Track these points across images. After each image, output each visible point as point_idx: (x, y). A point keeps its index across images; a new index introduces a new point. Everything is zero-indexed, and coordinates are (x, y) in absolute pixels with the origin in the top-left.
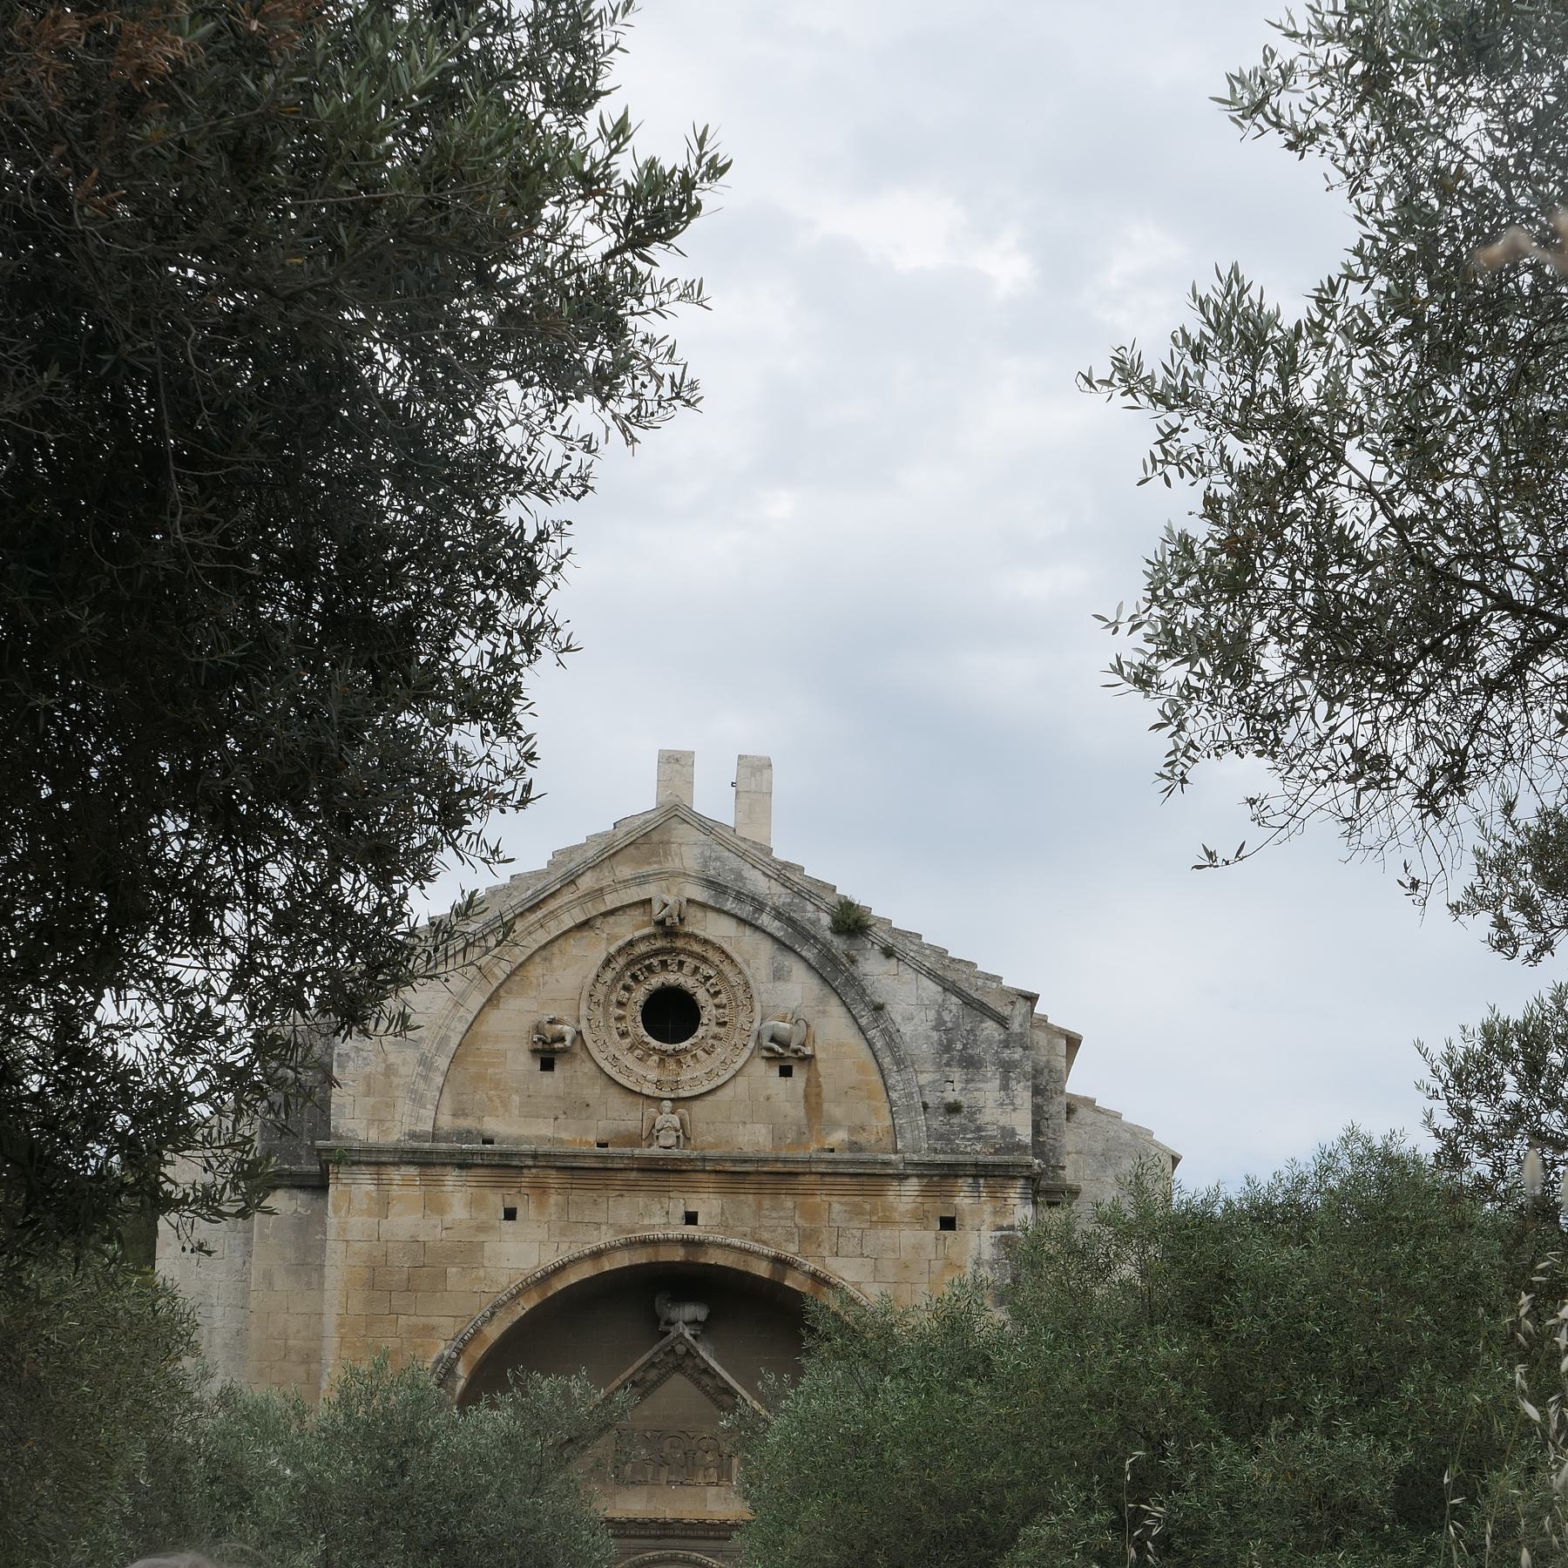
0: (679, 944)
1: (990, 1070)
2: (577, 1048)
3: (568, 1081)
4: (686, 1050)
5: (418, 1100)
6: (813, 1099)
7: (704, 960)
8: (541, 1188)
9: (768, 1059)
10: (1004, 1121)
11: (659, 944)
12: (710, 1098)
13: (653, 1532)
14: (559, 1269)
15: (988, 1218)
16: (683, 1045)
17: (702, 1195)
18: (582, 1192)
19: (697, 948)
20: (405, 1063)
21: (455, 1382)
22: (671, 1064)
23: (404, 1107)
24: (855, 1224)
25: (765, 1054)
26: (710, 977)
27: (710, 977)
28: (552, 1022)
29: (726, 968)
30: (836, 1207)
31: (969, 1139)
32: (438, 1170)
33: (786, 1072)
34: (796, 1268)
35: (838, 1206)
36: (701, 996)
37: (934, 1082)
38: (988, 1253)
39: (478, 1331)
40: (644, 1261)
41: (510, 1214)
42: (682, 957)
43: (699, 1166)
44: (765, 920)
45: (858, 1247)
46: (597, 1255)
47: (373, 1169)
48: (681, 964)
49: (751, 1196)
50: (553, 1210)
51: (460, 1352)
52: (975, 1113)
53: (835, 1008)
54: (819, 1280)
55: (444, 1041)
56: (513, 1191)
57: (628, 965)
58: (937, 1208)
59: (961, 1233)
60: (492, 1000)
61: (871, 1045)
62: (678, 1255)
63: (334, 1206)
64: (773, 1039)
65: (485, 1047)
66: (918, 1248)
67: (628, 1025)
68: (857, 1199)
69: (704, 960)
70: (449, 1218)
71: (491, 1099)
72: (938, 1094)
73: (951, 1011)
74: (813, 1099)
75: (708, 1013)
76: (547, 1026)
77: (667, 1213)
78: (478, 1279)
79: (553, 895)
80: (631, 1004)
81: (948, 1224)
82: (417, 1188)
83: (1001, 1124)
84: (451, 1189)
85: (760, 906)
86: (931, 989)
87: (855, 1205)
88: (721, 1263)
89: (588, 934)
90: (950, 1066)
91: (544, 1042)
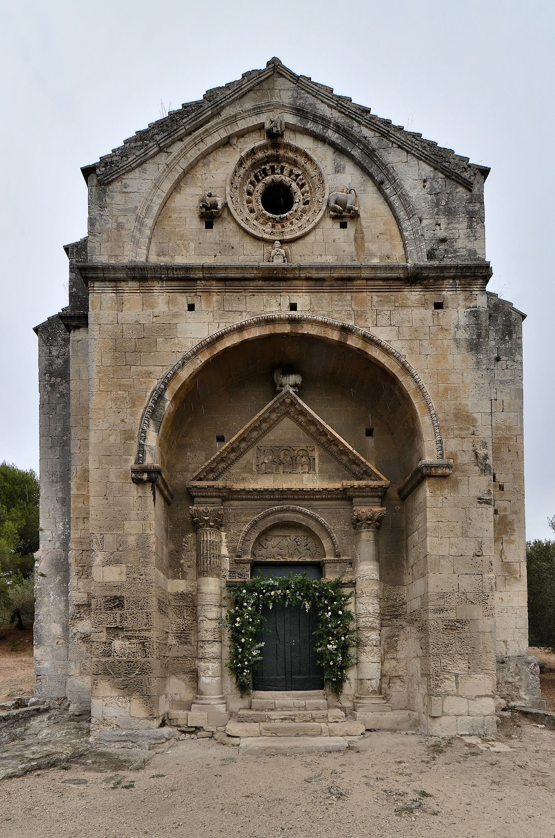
0: (281, 152)
2: (225, 215)
3: (221, 234)
4: (286, 219)
5: (136, 243)
7: (295, 163)
8: (209, 292)
10: (469, 246)
11: (270, 152)
12: (301, 242)
14: (220, 338)
15: (462, 303)
16: (285, 215)
17: (299, 294)
18: (231, 294)
19: (291, 155)
21: (164, 403)
22: (279, 226)
23: (128, 247)
24: (386, 308)
25: (332, 213)
26: (299, 175)
27: (299, 175)
28: (210, 195)
29: (308, 166)
30: (375, 299)
31: (449, 258)
32: (150, 283)
33: (343, 226)
34: (353, 333)
37: (429, 225)
38: (463, 321)
39: (175, 374)
40: (267, 333)
41: (191, 308)
42: (283, 164)
44: (331, 134)
45: (389, 321)
46: (241, 329)
47: (113, 284)
48: (282, 169)
49: (326, 294)
51: (166, 385)
52: (453, 242)
53: (371, 188)
54: (368, 339)
55: (149, 208)
57: (254, 166)
58: (432, 297)
59: (447, 310)
60: (176, 187)
61: (390, 205)
62: (286, 329)
64: (336, 203)
66: (422, 320)
67: (254, 205)
68: (387, 294)
69: (295, 163)
70: (156, 311)
72: (432, 232)
73: (438, 183)
75: (298, 197)
76: (207, 197)
77: (280, 305)
78: (174, 344)
79: (207, 121)
80: (255, 192)
81: (439, 306)
82: (138, 294)
83: (468, 248)
84: (158, 294)
86: (426, 170)
87: (386, 297)
88: (311, 332)
89: (229, 149)
90: (439, 215)
91: (207, 208)
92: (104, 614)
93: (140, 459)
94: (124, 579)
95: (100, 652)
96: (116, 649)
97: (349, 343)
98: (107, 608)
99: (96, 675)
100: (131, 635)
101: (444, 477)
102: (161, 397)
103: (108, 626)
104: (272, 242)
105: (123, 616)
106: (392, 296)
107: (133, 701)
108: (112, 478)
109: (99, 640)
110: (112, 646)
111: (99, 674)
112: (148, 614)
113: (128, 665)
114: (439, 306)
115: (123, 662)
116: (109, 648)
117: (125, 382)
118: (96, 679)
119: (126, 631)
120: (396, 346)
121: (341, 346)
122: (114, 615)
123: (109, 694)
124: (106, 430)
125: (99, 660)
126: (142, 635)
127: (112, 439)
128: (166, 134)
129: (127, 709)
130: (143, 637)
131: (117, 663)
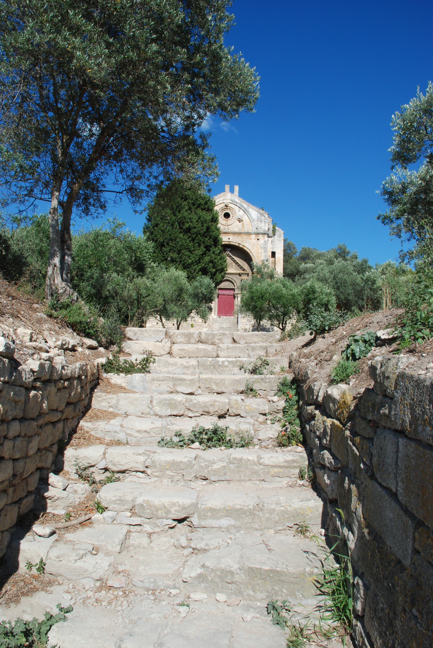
1: (263, 222)
6: (243, 225)
35: (245, 237)
36: (230, 213)
62: (227, 243)
74: (243, 225)
85: (237, 203)
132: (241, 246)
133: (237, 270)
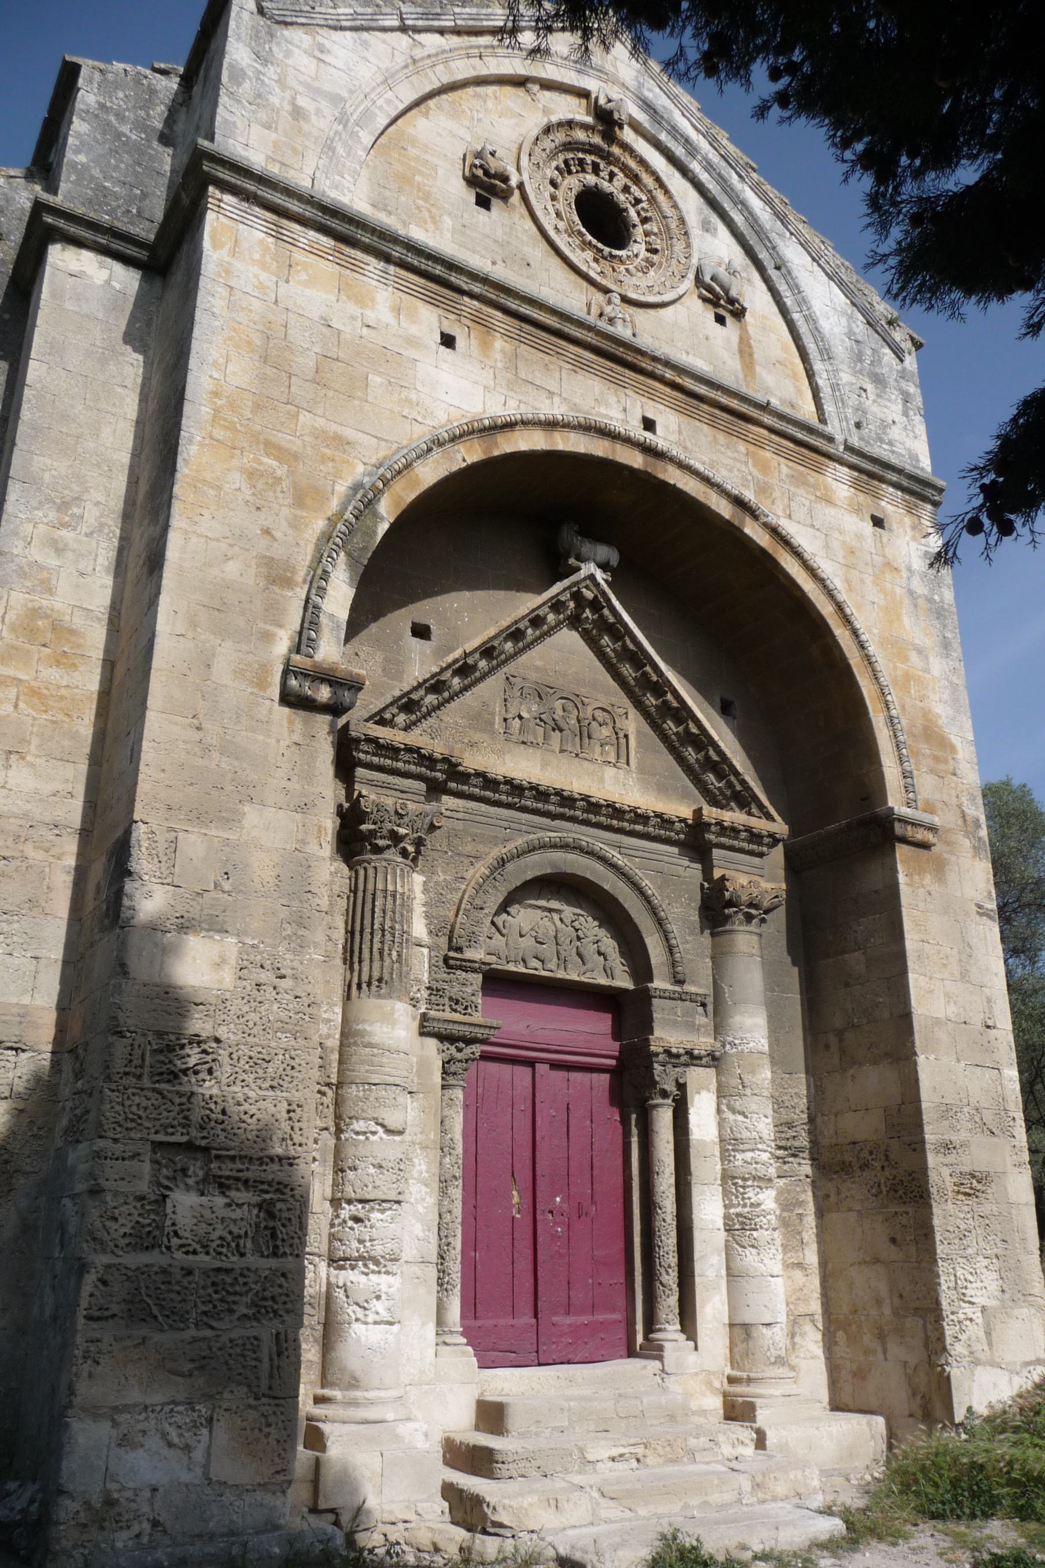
9: (705, 300)
11: (597, 140)
13: (552, 808)
14: (509, 426)
18: (533, 350)
19: (632, 164)
20: (318, 111)
33: (720, 320)
42: (616, 170)
43: (660, 369)
46: (551, 425)
48: (612, 175)
50: (498, 356)
56: (452, 317)
57: (569, 146)
63: (213, 237)
65: (413, 151)
67: (561, 206)
69: (636, 179)
70: (371, 316)
71: (418, 208)
78: (408, 401)
87: (801, 473)
88: (680, 485)
91: (486, 173)
92: (149, 1094)
93: (303, 642)
94: (228, 978)
95: (123, 1230)
96: (179, 1219)
97: (747, 530)
98: (162, 1074)
99: (99, 1319)
100: (234, 1174)
101: (925, 846)
102: (370, 504)
103: (161, 1137)
104: (606, 291)
105: (213, 1106)
106: (813, 477)
107: (222, 1423)
108: (222, 672)
109: (123, 1187)
110: (169, 1209)
111: (106, 1318)
112: (294, 1107)
113: (214, 1284)
114: (878, 522)
115: (197, 1272)
116: (152, 1216)
117: (283, 439)
118: (97, 1335)
119: (218, 1157)
120: (826, 568)
121: (732, 533)
122: (184, 1100)
123: (135, 1396)
124: (217, 540)
125: (117, 1261)
126: (270, 1178)
127: (232, 569)
128: (419, 10)
129: (198, 1455)
130: (270, 1184)
131: (177, 1274)
132: (752, 530)
133: (662, 789)
